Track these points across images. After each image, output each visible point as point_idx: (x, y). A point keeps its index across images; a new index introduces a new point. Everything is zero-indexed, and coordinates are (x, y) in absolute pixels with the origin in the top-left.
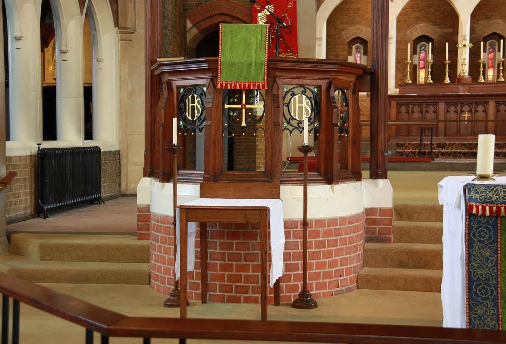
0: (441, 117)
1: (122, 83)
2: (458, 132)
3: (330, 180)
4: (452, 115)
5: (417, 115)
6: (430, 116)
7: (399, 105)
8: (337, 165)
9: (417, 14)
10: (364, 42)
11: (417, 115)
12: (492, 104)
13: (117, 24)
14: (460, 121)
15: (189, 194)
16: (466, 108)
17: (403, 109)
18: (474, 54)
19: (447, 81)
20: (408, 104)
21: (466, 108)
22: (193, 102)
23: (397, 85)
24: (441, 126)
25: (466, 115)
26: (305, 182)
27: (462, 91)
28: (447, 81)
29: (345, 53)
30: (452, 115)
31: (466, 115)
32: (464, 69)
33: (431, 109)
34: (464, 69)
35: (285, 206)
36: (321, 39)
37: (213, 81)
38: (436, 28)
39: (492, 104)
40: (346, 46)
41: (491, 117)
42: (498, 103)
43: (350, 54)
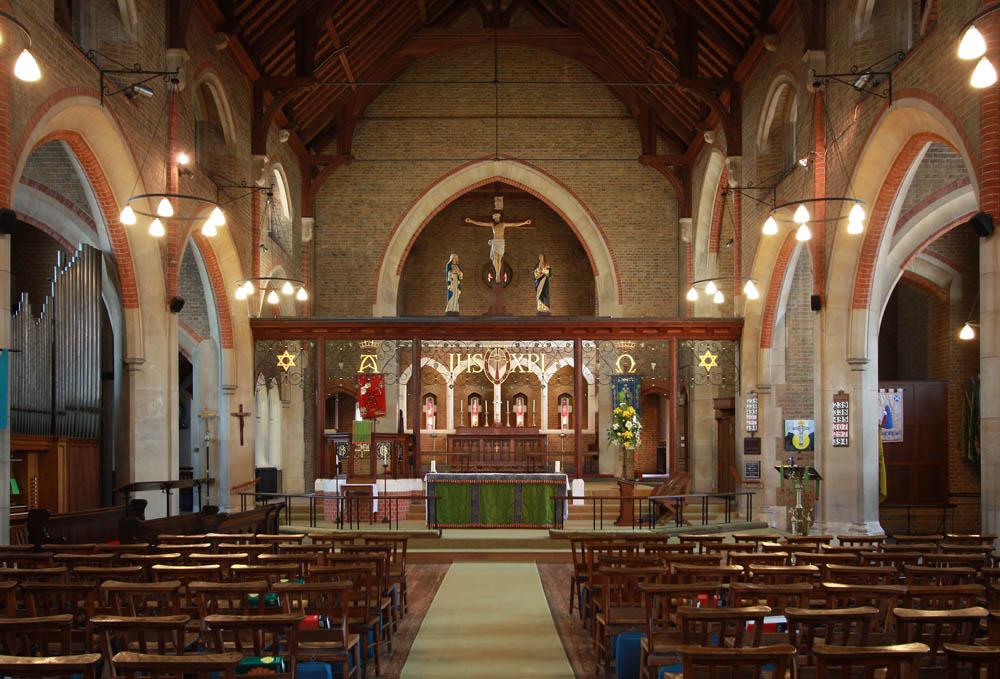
0: (481, 449)
1: (283, 431)
2: (492, 459)
3: (395, 477)
4: (489, 448)
5: (466, 448)
6: (474, 449)
7: (454, 441)
8: (398, 471)
11: (466, 448)
12: (512, 442)
14: (493, 452)
15: (342, 482)
16: (497, 444)
17: (457, 444)
18: (503, 407)
19: (487, 425)
20: (460, 441)
21: (497, 444)
23: (455, 428)
24: (482, 455)
25: (497, 448)
26: (385, 478)
27: (497, 432)
28: (487, 425)
30: (489, 448)
31: (497, 448)
32: (498, 418)
33: (475, 444)
34: (498, 418)
35: (378, 487)
36: (402, 396)
37: (351, 441)
39: (512, 442)
41: (512, 450)
42: (516, 441)
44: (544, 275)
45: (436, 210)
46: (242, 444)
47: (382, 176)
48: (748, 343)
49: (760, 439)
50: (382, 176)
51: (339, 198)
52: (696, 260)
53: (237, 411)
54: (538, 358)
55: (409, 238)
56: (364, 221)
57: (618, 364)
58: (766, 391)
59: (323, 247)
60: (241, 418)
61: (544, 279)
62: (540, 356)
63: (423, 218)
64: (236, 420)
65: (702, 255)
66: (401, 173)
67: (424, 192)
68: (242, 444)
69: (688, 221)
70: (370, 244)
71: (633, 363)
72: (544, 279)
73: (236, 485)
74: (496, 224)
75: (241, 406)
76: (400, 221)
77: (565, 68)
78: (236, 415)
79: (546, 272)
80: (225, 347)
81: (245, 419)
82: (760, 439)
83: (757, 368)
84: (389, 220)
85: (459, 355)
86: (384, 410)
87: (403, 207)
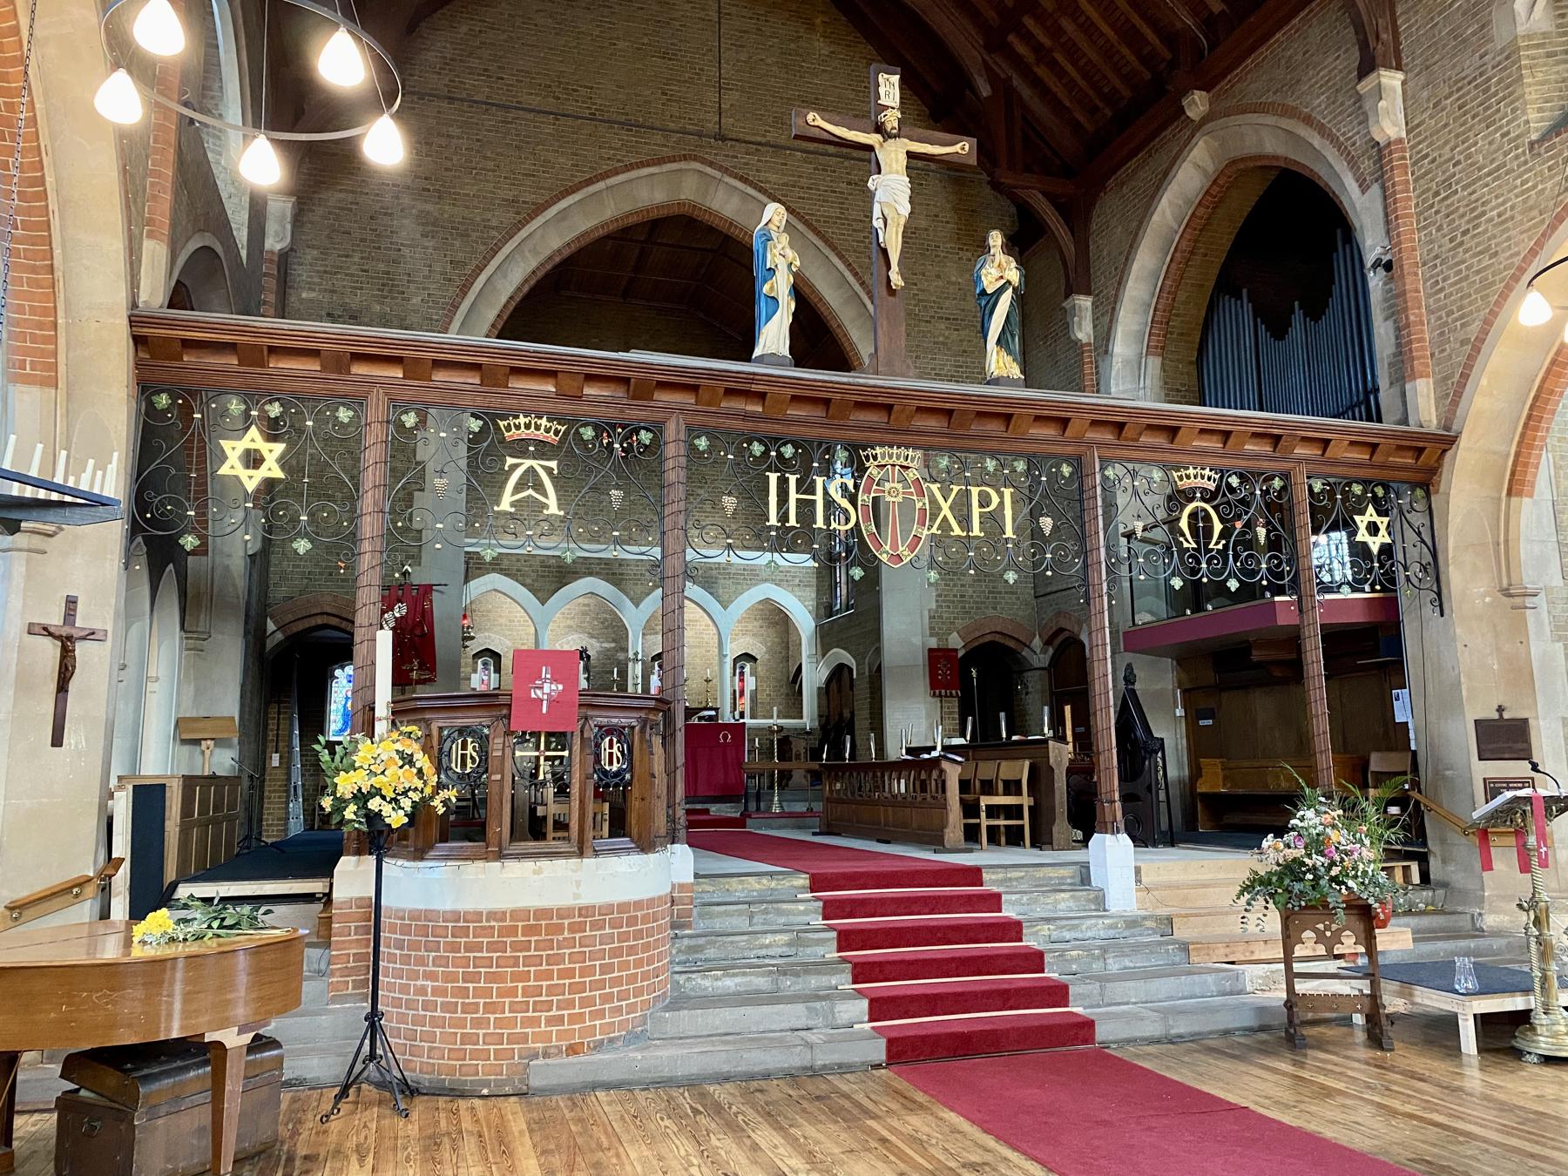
9: (570, 622)
10: (496, 656)
13: (182, 627)
22: (611, 747)
29: (469, 669)
38: (593, 641)
40: (470, 660)
43: (475, 671)
44: (1009, 282)
45: (559, 251)
46: (57, 741)
47: (449, 164)
48: (1464, 489)
49: (1525, 721)
50: (449, 164)
51: (350, 198)
52: (1113, 373)
53: (55, 619)
54: (995, 500)
55: (504, 300)
56: (406, 251)
57: (1184, 524)
58: (1529, 602)
59: (304, 295)
60: (67, 646)
61: (1009, 292)
62: (1001, 495)
63: (534, 264)
64: (52, 649)
65: (1126, 362)
66: (491, 165)
67: (540, 209)
68: (57, 741)
69: (1084, 302)
70: (416, 300)
71: (1218, 527)
72: (1009, 292)
73: (23, 893)
74: (887, 136)
75: (71, 602)
76: (487, 261)
77: (818, 21)
78: (47, 631)
79: (1014, 275)
80: (28, 380)
81: (81, 649)
82: (1525, 721)
83: (1502, 549)
84: (460, 256)
85: (793, 479)
86: (433, 669)
87: (494, 233)
